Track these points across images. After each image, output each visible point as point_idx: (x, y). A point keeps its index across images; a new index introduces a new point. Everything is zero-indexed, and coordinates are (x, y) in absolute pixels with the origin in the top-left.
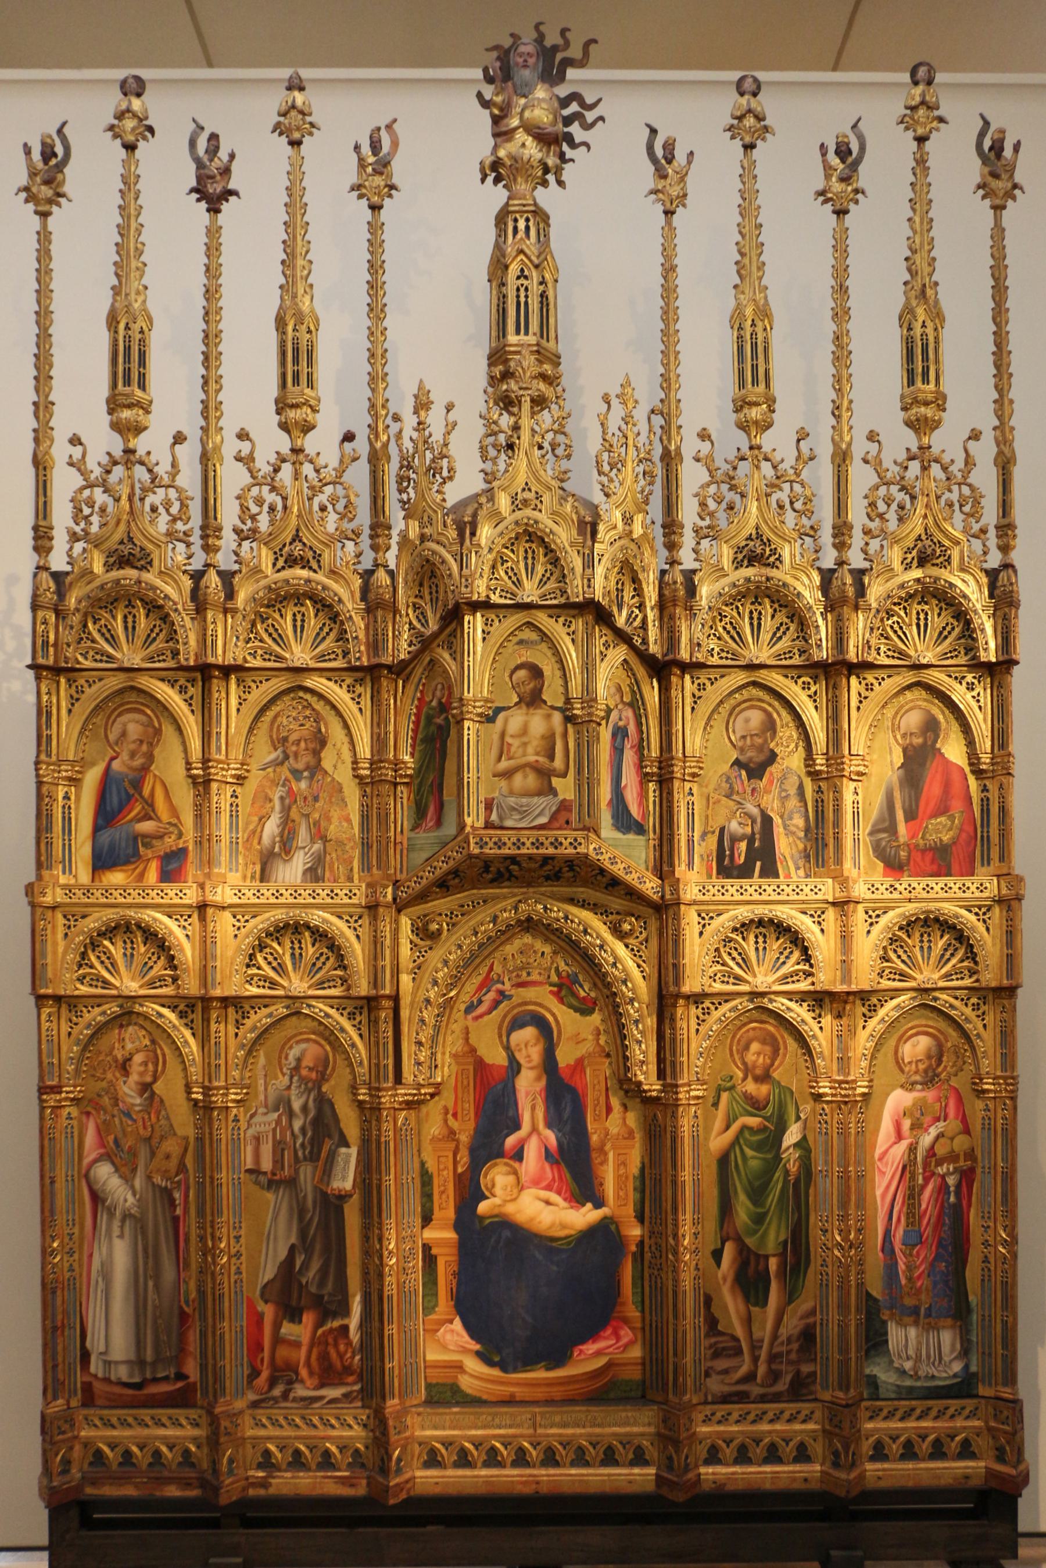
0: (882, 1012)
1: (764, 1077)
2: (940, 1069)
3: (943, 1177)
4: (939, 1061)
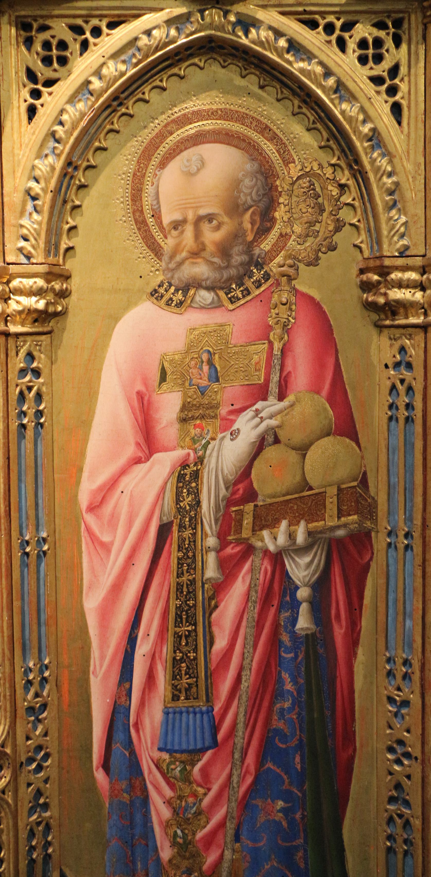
0: (81, 66)
3: (277, 559)
4: (265, 221)
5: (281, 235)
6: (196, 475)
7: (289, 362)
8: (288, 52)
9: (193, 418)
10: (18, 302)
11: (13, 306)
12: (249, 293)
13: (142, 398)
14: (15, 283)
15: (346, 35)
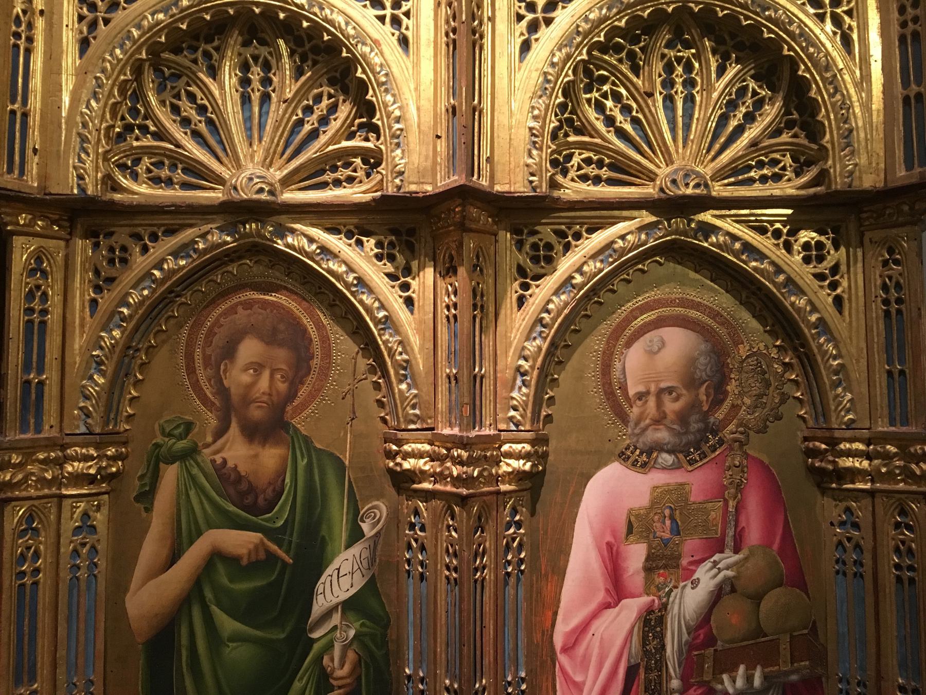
0: (565, 265)
1: (271, 427)
2: (720, 414)
4: (719, 395)
5: (733, 406)
6: (661, 621)
7: (743, 519)
8: (743, 254)
9: (658, 568)
10: (508, 465)
11: (504, 468)
12: (706, 457)
13: (612, 549)
14: (505, 448)
15: (792, 239)
